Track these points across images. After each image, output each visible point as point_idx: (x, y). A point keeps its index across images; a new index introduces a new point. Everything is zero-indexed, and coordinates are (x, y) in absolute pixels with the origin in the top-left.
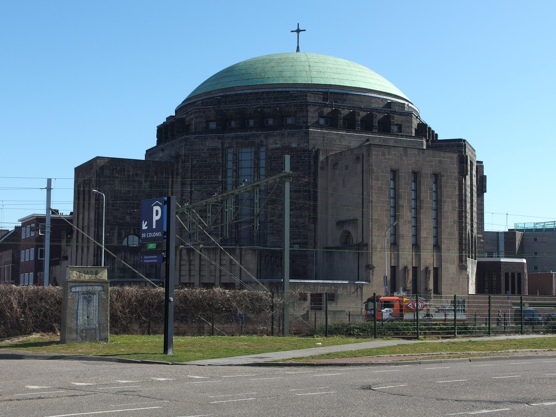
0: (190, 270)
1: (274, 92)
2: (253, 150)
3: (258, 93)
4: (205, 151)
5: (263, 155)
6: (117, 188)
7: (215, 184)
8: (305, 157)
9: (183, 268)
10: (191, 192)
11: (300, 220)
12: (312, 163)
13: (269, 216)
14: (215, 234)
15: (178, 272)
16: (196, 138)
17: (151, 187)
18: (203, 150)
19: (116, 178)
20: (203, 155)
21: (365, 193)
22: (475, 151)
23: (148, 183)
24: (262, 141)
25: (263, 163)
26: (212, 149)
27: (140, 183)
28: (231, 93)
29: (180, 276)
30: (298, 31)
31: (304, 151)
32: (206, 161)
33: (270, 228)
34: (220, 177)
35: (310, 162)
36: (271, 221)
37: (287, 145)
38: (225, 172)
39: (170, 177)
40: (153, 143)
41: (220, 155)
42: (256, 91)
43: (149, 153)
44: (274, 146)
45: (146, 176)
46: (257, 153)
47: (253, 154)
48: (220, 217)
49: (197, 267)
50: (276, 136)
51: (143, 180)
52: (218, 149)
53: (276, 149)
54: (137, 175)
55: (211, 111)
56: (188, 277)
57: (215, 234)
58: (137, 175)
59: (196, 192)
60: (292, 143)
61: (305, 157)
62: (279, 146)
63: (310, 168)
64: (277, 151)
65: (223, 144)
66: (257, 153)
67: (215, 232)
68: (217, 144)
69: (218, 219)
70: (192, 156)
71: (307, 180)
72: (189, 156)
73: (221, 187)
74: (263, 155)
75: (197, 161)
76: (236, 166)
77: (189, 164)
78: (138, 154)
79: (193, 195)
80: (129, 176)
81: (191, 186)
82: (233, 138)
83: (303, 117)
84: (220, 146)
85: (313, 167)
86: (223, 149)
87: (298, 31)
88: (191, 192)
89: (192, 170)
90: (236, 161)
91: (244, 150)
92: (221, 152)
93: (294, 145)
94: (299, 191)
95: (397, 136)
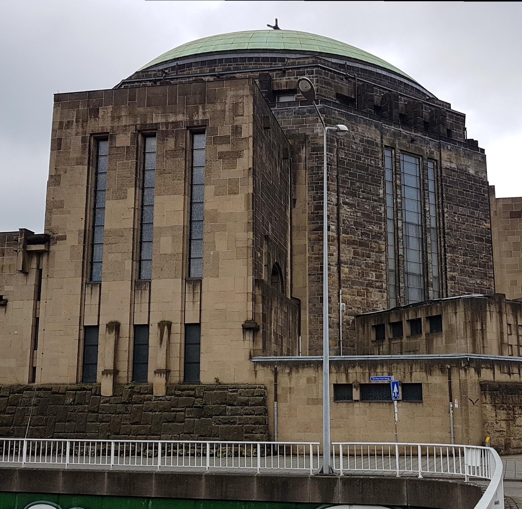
4: (357, 141)
5: (431, 174)
7: (374, 200)
11: (485, 283)
13: (448, 270)
14: (378, 287)
18: (354, 139)
20: (354, 147)
25: (431, 187)
26: (368, 142)
33: (451, 288)
34: (381, 192)
36: (453, 278)
41: (380, 155)
48: (383, 259)
50: (450, 150)
53: (451, 170)
57: (378, 287)
59: (346, 207)
62: (454, 166)
64: (453, 173)
66: (425, 168)
67: (377, 284)
68: (373, 134)
69: (381, 262)
73: (383, 208)
79: (342, 211)
81: (338, 195)
82: (394, 133)
90: (397, 172)
91: (407, 158)
93: (471, 171)
94: (482, 240)
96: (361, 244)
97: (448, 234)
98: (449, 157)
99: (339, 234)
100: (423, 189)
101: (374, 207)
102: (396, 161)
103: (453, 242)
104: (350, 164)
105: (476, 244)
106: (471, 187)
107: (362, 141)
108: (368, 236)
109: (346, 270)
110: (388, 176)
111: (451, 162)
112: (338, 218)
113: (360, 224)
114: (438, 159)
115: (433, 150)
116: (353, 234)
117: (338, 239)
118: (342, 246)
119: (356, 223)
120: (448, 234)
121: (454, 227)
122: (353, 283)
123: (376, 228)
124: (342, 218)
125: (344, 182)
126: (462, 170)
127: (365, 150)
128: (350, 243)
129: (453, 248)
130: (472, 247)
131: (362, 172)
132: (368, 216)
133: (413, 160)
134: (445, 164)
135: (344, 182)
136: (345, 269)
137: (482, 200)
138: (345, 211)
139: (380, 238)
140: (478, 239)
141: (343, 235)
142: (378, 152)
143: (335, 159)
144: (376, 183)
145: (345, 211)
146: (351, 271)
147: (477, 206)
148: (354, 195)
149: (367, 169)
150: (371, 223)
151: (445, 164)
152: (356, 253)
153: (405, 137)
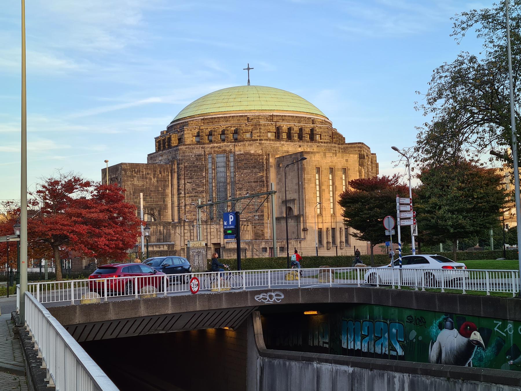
0: (191, 236)
1: (237, 116)
2: (225, 155)
3: (226, 117)
5: (232, 159)
6: (136, 183)
9: (186, 235)
10: (185, 184)
12: (265, 163)
16: (186, 148)
17: (157, 181)
19: (135, 176)
21: (300, 183)
22: (369, 148)
23: (156, 179)
25: (232, 164)
26: (198, 155)
27: (151, 179)
28: (208, 117)
30: (248, 69)
31: (259, 155)
32: (194, 163)
34: (204, 174)
35: (263, 163)
38: (207, 170)
39: (170, 174)
40: (153, 149)
42: (225, 115)
43: (151, 157)
45: (154, 175)
46: (227, 157)
47: (225, 158)
51: (152, 177)
54: (148, 174)
58: (148, 174)
62: (242, 152)
63: (263, 167)
66: (227, 157)
71: (261, 174)
72: (182, 160)
74: (232, 159)
75: (188, 163)
77: (182, 166)
78: (141, 158)
80: (143, 175)
82: (211, 148)
83: (257, 133)
84: (203, 153)
85: (265, 166)
86: (205, 155)
87: (248, 69)
88: (185, 184)
93: (252, 152)
94: (257, 182)
95: (319, 142)
96: (195, 196)
97: (238, 183)
99: (185, 194)
100: (227, 166)
101: (200, 181)
102: (213, 158)
103: (240, 186)
104: (190, 167)
105: (254, 184)
106: (252, 159)
107: (195, 156)
108: (198, 192)
109: (189, 207)
110: (210, 165)
112: (185, 189)
113: (194, 189)
116: (191, 193)
117: (185, 197)
118: (187, 199)
119: (192, 189)
120: (238, 183)
121: (241, 179)
122: (191, 212)
123: (201, 189)
124: (186, 188)
125: (187, 174)
127: (197, 159)
128: (190, 197)
129: (240, 189)
130: (251, 186)
132: (198, 185)
133: (223, 155)
134: (237, 153)
135: (187, 174)
136: (188, 207)
138: (188, 186)
139: (203, 192)
140: (254, 182)
141: (187, 195)
144: (202, 171)
145: (188, 186)
146: (190, 208)
147: (255, 167)
148: (191, 178)
150: (199, 187)
151: (237, 153)
152: (192, 200)
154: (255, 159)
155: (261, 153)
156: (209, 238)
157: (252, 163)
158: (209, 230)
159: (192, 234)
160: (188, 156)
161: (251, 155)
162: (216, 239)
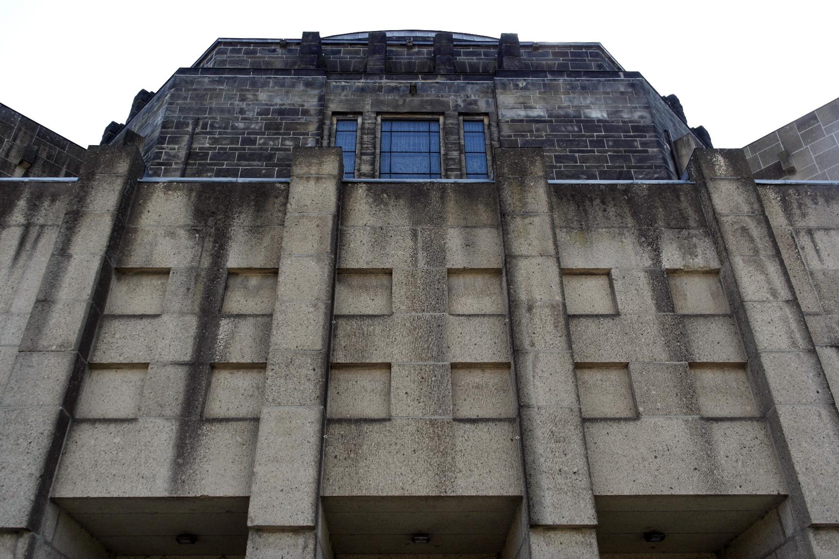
0: (202, 366)
4: (250, 115)
8: (643, 144)
15: (54, 371)
20: (241, 125)
24: (475, 102)
26: (281, 112)
29: (67, 420)
32: (253, 142)
35: (665, 162)
37: (571, 111)
41: (312, 128)
44: (522, 113)
49: (299, 328)
50: (525, 88)
52: (305, 112)
55: (274, 51)
56: (162, 435)
60: (588, 107)
61: (643, 144)
64: (534, 126)
65: (323, 101)
70: (196, 124)
72: (180, 125)
75: (215, 141)
76: (373, 163)
82: (363, 90)
84: (311, 103)
86: (321, 112)
89: (186, 163)
92: (315, 120)
93: (596, 114)
98: (521, 100)
106: (599, 143)
111: (527, 107)
114: (491, 109)
115: (473, 98)
126: (567, 116)
127: (273, 127)
131: (256, 163)
137: (641, 160)
142: (306, 124)
143: (183, 154)
149: (270, 157)
151: (508, 114)
153: (396, 89)
154: (617, 143)
155: (648, 121)
156: (548, 385)
157: (599, 159)
158: (536, 279)
159: (237, 341)
160: (222, 111)
161: (590, 125)
162: (669, 430)
